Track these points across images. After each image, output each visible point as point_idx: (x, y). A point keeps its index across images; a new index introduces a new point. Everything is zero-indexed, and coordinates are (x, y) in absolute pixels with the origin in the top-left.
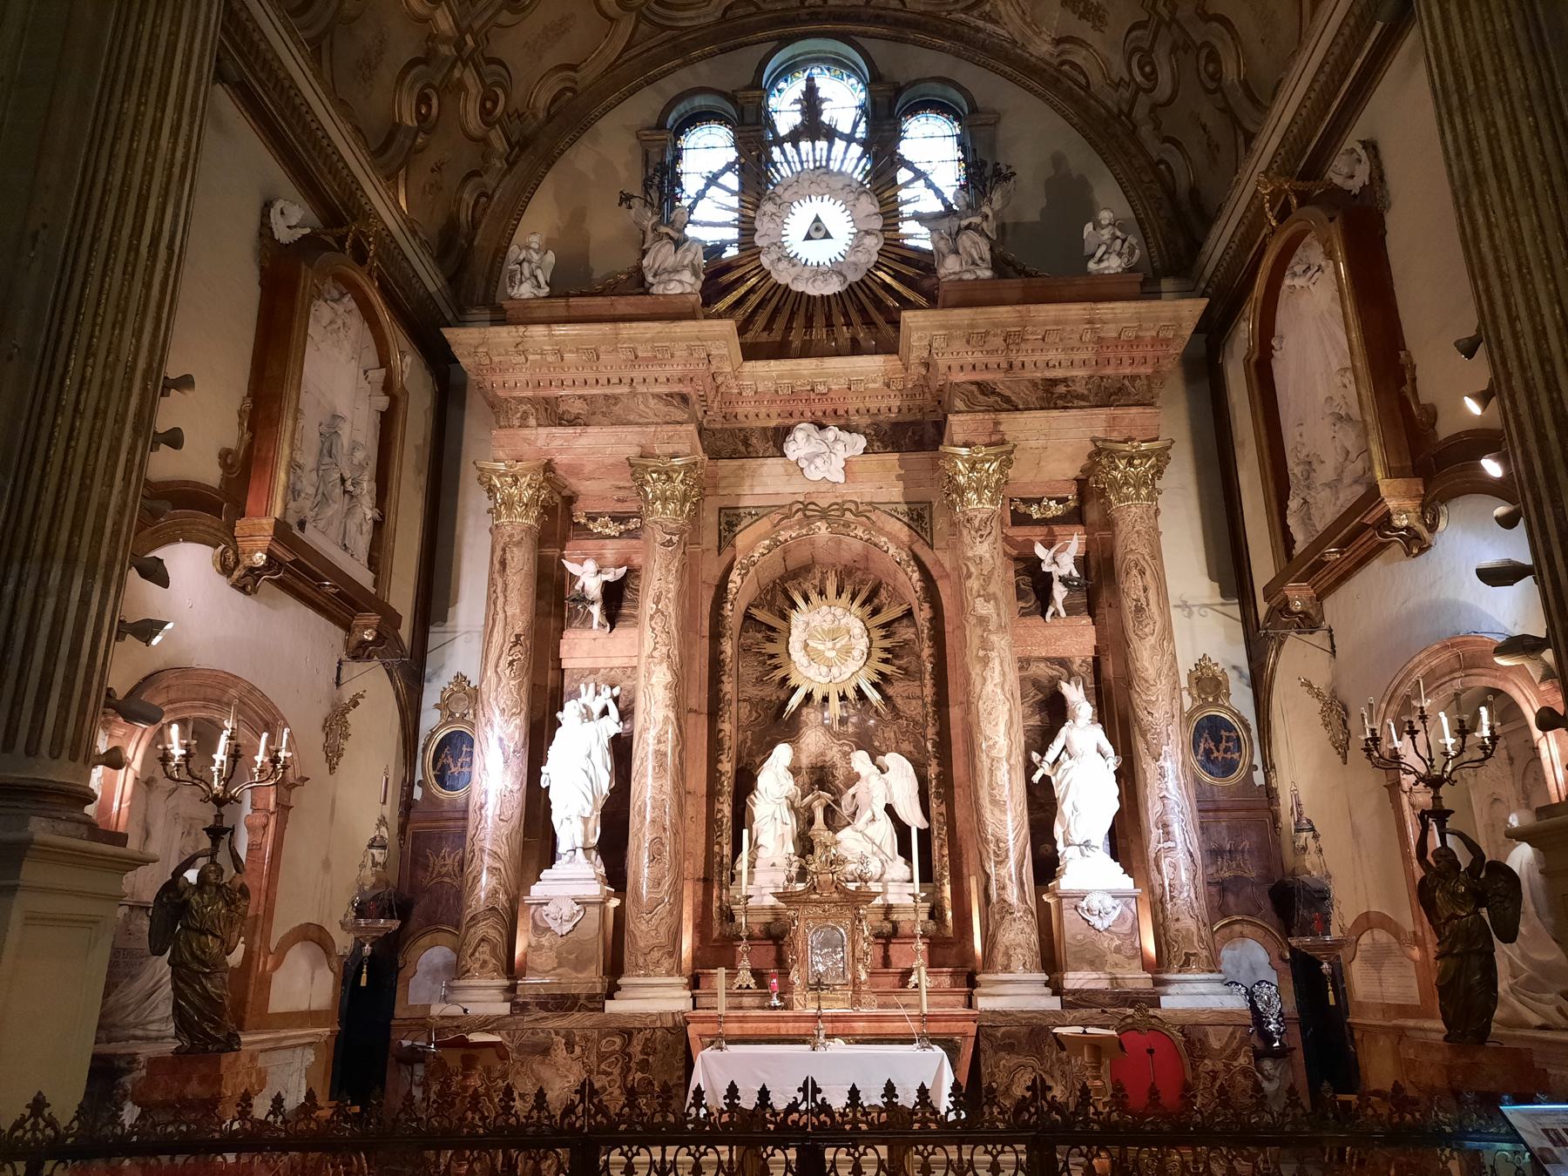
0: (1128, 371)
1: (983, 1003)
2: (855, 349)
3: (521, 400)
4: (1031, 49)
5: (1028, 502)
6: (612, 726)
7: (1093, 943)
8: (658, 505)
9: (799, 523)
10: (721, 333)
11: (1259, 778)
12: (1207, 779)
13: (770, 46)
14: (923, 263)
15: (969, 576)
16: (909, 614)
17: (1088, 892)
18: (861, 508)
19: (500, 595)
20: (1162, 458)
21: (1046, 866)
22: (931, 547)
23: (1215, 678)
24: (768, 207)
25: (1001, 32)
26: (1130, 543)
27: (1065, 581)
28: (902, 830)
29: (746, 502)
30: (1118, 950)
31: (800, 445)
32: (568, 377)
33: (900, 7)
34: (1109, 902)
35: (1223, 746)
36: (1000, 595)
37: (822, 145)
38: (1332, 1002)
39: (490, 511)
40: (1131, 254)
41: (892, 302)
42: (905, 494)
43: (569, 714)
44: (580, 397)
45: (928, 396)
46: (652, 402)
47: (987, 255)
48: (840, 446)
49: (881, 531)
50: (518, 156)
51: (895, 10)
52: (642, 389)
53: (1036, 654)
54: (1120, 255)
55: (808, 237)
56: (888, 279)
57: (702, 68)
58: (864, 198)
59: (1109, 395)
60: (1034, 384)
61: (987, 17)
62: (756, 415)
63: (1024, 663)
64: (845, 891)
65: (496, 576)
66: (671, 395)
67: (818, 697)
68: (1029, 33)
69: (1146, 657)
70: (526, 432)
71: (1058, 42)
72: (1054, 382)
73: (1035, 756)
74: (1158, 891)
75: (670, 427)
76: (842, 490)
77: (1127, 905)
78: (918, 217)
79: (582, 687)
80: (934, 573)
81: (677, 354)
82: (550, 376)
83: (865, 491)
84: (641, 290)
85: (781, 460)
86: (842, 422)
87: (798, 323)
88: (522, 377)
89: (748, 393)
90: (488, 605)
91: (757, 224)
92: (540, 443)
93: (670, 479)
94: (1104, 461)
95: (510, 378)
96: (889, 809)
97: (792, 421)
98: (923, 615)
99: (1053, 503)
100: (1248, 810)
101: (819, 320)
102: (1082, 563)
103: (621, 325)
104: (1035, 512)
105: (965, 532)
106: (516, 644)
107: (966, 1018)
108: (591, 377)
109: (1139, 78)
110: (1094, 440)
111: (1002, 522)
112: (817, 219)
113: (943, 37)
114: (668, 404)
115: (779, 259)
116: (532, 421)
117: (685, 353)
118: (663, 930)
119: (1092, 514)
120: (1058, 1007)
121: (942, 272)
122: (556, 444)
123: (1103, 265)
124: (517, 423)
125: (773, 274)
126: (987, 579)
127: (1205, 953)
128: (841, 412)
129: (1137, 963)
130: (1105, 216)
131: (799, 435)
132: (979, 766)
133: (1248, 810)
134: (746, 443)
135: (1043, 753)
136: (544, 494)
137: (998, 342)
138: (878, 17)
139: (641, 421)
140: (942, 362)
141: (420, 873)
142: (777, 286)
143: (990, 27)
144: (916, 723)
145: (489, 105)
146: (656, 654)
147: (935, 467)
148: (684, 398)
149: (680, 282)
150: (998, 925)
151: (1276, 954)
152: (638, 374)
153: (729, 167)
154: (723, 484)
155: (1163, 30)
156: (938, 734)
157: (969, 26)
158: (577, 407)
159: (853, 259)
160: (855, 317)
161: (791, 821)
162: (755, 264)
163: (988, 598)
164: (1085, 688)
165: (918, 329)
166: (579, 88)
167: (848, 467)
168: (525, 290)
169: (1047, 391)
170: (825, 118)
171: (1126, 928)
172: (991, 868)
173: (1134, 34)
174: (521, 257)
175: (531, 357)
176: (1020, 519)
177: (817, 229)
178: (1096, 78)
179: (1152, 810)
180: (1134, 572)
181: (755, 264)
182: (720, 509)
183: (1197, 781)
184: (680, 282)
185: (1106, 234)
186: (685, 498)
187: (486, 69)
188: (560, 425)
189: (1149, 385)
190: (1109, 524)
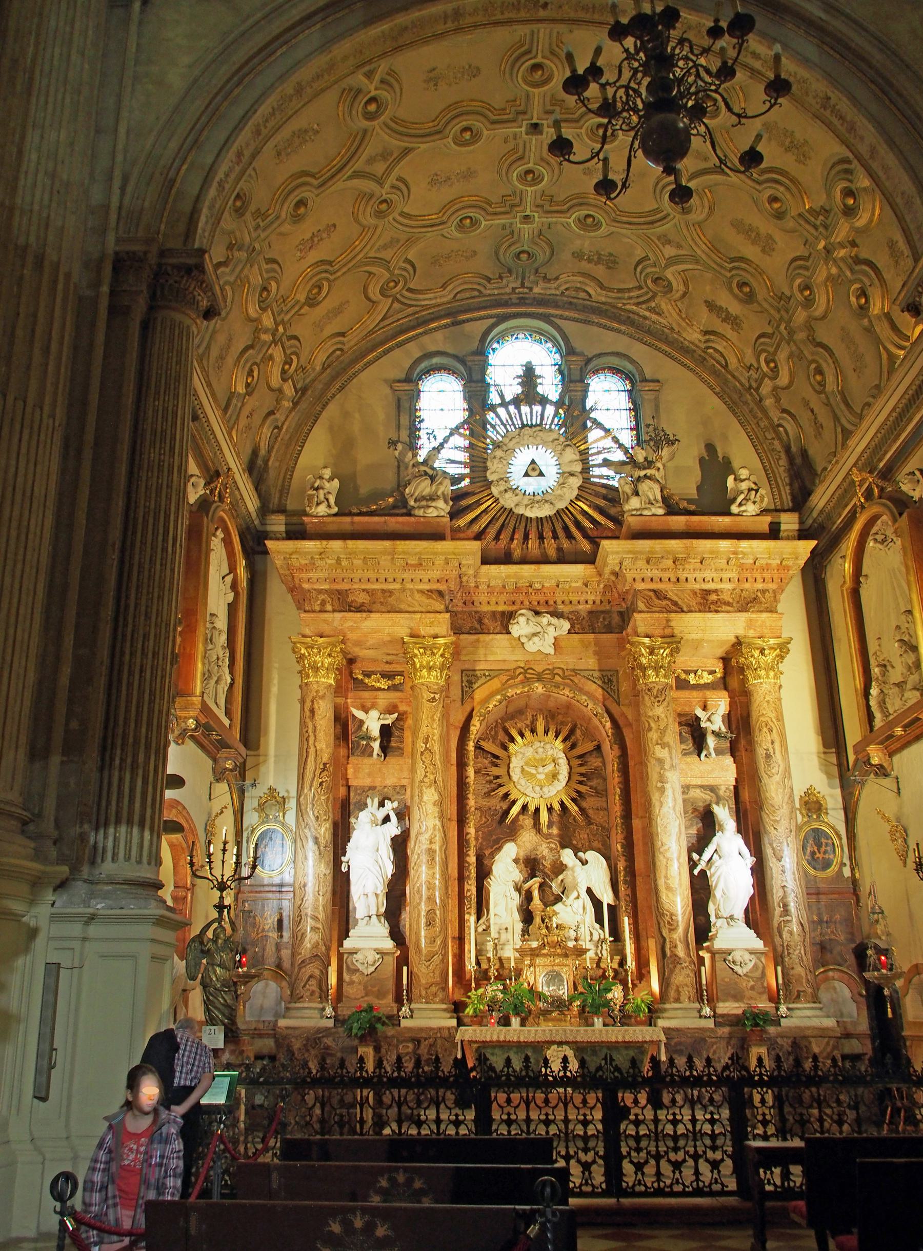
2: (562, 559)
3: (320, 591)
4: (684, 335)
5: (687, 672)
7: (736, 983)
8: (424, 672)
9: (522, 682)
13: (491, 321)
14: (612, 496)
17: (733, 950)
19: (311, 734)
23: (818, 802)
25: (661, 320)
29: (481, 666)
30: (752, 988)
31: (521, 627)
32: (356, 576)
34: (747, 956)
35: (823, 849)
37: (537, 408)
38: (890, 1015)
39: (300, 672)
41: (587, 524)
42: (600, 664)
44: (364, 590)
46: (417, 596)
48: (551, 629)
49: (581, 690)
50: (300, 398)
53: (694, 783)
55: (526, 475)
56: (585, 508)
57: (439, 335)
58: (568, 450)
62: (487, 604)
63: (686, 788)
66: (431, 591)
68: (684, 324)
70: (326, 615)
71: (706, 333)
73: (695, 856)
74: (780, 949)
75: (432, 615)
77: (759, 959)
78: (606, 463)
80: (621, 723)
81: (437, 562)
82: (343, 576)
83: (568, 661)
84: (404, 511)
85: (507, 636)
87: (519, 536)
89: (483, 587)
90: (301, 741)
91: (489, 464)
92: (336, 624)
93: (433, 654)
98: (611, 753)
99: (705, 674)
100: (839, 893)
101: (533, 536)
102: (728, 719)
106: (323, 770)
108: (372, 575)
109: (765, 369)
112: (533, 462)
113: (620, 322)
114: (430, 597)
115: (506, 491)
116: (329, 607)
118: (437, 973)
120: (712, 1026)
122: (349, 624)
124: (317, 608)
125: (502, 501)
127: (810, 990)
129: (765, 997)
131: (522, 620)
132: (658, 863)
133: (839, 893)
134: (480, 621)
135: (700, 855)
138: (571, 303)
142: (503, 509)
143: (654, 317)
146: (426, 780)
147: (621, 644)
148: (440, 593)
149: (436, 508)
151: (855, 992)
152: (407, 576)
154: (464, 652)
156: (625, 838)
157: (638, 315)
158: (362, 598)
159: (559, 492)
160: (561, 534)
162: (488, 492)
164: (730, 808)
165: (613, 553)
166: (346, 348)
167: (556, 644)
168: (322, 510)
170: (540, 389)
171: (758, 974)
172: (665, 933)
173: (762, 340)
177: (533, 469)
178: (733, 363)
179: (776, 895)
182: (462, 671)
183: (806, 874)
184: (436, 508)
186: (442, 668)
187: (288, 344)
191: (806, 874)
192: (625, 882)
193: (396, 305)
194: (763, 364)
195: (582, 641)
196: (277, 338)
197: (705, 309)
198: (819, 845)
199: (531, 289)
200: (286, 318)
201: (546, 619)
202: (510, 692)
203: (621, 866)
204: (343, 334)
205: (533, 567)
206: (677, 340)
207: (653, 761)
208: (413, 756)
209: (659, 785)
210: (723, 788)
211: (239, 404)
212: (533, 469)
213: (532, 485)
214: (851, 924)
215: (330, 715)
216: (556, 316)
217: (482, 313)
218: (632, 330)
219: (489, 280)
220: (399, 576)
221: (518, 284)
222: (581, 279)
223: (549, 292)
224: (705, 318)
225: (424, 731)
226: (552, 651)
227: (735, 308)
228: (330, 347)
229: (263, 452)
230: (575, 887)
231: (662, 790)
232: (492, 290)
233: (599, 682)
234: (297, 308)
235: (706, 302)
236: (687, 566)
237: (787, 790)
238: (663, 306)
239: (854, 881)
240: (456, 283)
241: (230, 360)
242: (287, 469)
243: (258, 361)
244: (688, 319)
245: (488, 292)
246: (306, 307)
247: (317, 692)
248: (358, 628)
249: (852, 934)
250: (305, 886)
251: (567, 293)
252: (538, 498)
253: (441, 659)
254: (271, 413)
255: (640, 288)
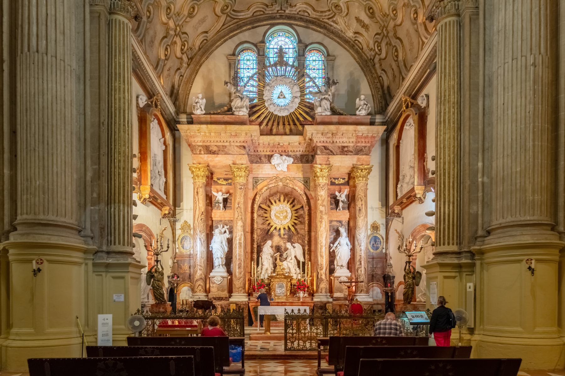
0: (364, 145)
1: (315, 300)
2: (292, 133)
3: (199, 146)
6: (227, 235)
10: (255, 129)
11: (384, 251)
12: (372, 251)
13: (268, 26)
14: (311, 107)
15: (319, 200)
16: (302, 207)
18: (291, 179)
20: (370, 170)
21: (332, 271)
22: (309, 190)
24: (268, 88)
26: (360, 192)
27: (343, 202)
28: (298, 262)
31: (276, 160)
32: (212, 140)
33: (308, 15)
35: (377, 243)
36: (326, 205)
37: (284, 67)
39: (192, 178)
40: (368, 109)
41: (301, 119)
43: (216, 232)
44: (216, 146)
45: (310, 148)
46: (236, 148)
47: (329, 107)
51: (307, 16)
52: (232, 144)
54: (365, 110)
59: (358, 151)
60: (339, 147)
61: (334, 22)
64: (285, 276)
65: (196, 196)
67: (278, 228)
69: (361, 222)
72: (344, 147)
73: (332, 245)
75: (241, 156)
76: (286, 173)
78: (310, 93)
79: (219, 225)
80: (310, 197)
81: (243, 134)
82: (207, 140)
86: (287, 154)
87: (275, 124)
88: (200, 139)
90: (194, 204)
91: (264, 93)
94: (355, 170)
95: (196, 139)
96: (295, 257)
97: (273, 153)
101: (281, 123)
102: (348, 196)
103: (227, 126)
104: (337, 182)
105: (318, 188)
107: (311, 303)
108: (219, 140)
109: (377, 50)
110: (353, 165)
111: (328, 184)
112: (281, 92)
116: (202, 152)
117: (244, 134)
119: (351, 183)
121: (316, 112)
123: (361, 112)
124: (198, 153)
126: (323, 201)
128: (287, 151)
130: (363, 97)
135: (333, 244)
136: (207, 173)
137: (330, 135)
138: (301, 18)
139: (233, 153)
140: (315, 140)
141: (180, 269)
143: (335, 25)
144: (303, 235)
145: (183, 47)
147: (312, 167)
148: (244, 147)
150: (320, 283)
152: (232, 140)
153: (255, 74)
155: (384, 38)
158: (215, 149)
159: (291, 105)
160: (291, 123)
161: (271, 259)
163: (323, 206)
169: (342, 150)
170: (285, 59)
173: (377, 36)
174: (196, 101)
175: (202, 134)
176: (333, 184)
177: (281, 95)
180: (360, 200)
181: (263, 105)
185: (362, 103)
188: (211, 154)
189: (369, 149)
190: (355, 186)
191: (369, 251)
192: (308, 254)
193: (228, 18)
194: (376, 48)
195: (297, 166)
196: (177, 33)
197: (355, 21)
198: (376, 242)
199: (285, 11)
200: (180, 23)
201: (284, 157)
202: (270, 186)
203: (306, 248)
204: (206, 32)
205: (280, 137)
206: (343, 36)
207: (319, 211)
208: (234, 210)
209: (320, 220)
210: (344, 221)
211: (163, 64)
212: (281, 96)
213: (282, 102)
214: (384, 268)
215: (204, 194)
216: (294, 24)
217: (265, 23)
218: (325, 31)
219: (267, 6)
220: (229, 140)
221: (279, 8)
222: (305, 6)
223: (292, 13)
224: (355, 26)
225: (238, 200)
226: (286, 170)
227: (367, 20)
228: (201, 38)
229: (176, 87)
230: (291, 255)
231: (321, 222)
232: (269, 11)
233: (303, 182)
234: (184, 19)
235: (356, 17)
236: (337, 136)
237: (365, 222)
238: (338, 19)
239: (386, 254)
240: (254, 7)
241: (157, 43)
242: (186, 94)
243: (169, 44)
244: (348, 26)
245: (267, 12)
246: (188, 18)
247: (199, 185)
248: (213, 161)
249: (383, 272)
250: (197, 255)
251: (300, 13)
252: (283, 108)
253: (244, 173)
254: (179, 69)
255: (329, 10)
